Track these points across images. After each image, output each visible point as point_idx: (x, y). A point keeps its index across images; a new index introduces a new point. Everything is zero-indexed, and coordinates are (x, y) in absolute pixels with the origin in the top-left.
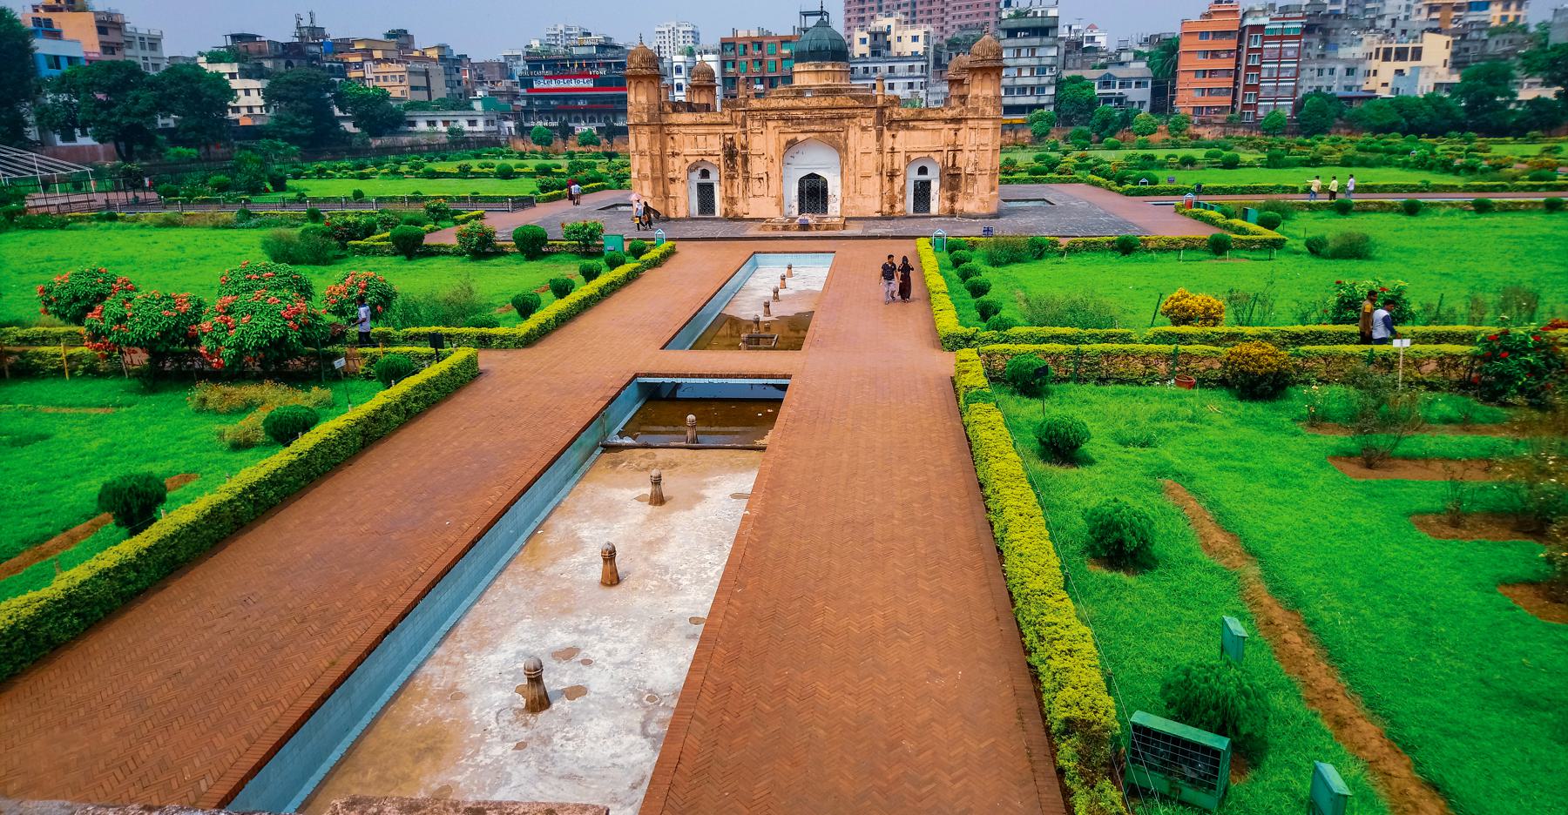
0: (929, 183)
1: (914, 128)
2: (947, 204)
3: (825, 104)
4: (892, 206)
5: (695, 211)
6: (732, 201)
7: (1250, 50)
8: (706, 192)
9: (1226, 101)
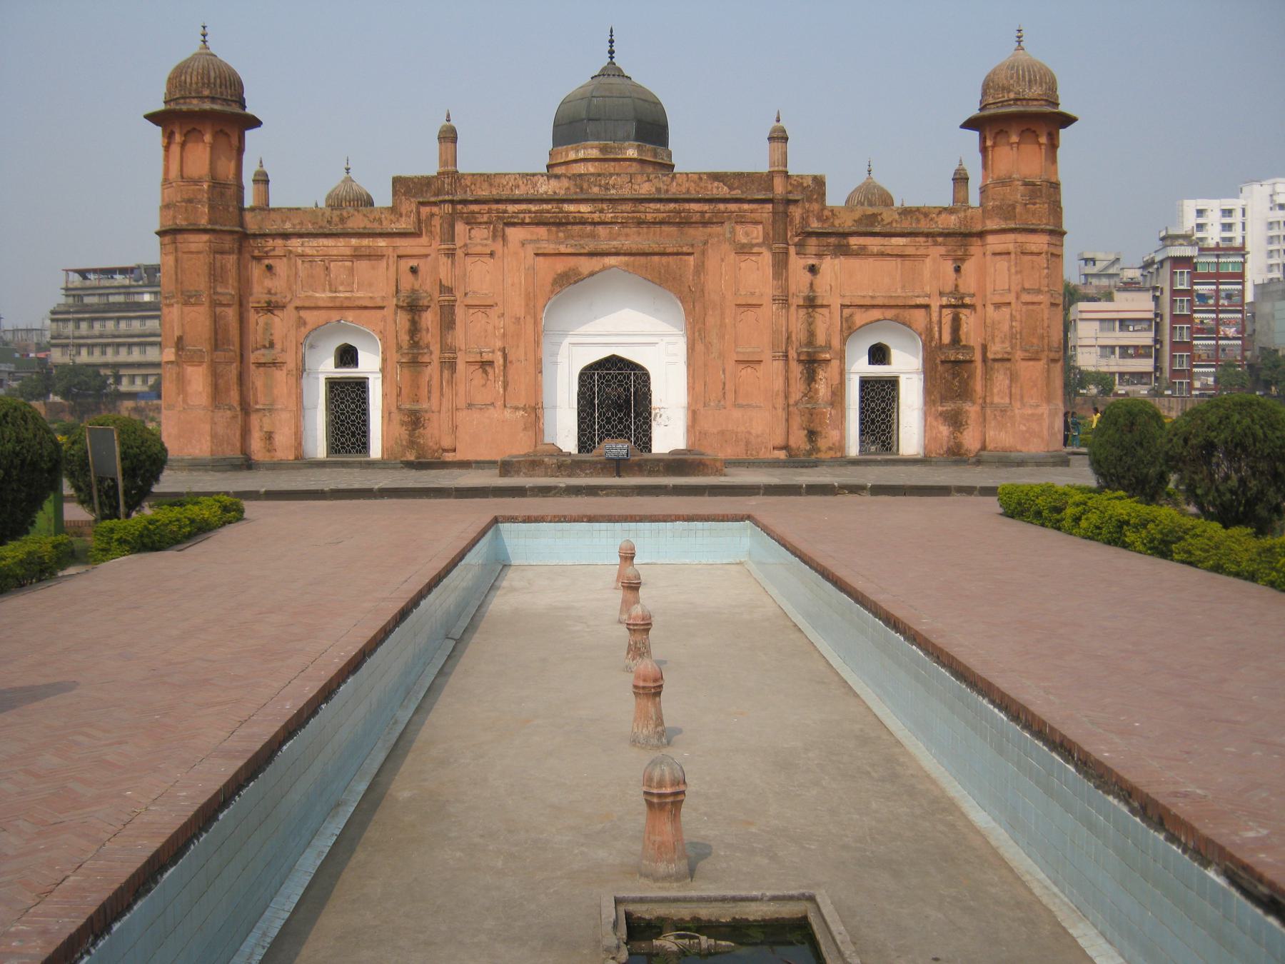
0: (891, 384)
1: (862, 252)
2: (944, 430)
3: (645, 189)
4: (812, 435)
5: (318, 446)
6: (412, 421)
7: (1175, 293)
8: (347, 399)
9: (1146, 365)
